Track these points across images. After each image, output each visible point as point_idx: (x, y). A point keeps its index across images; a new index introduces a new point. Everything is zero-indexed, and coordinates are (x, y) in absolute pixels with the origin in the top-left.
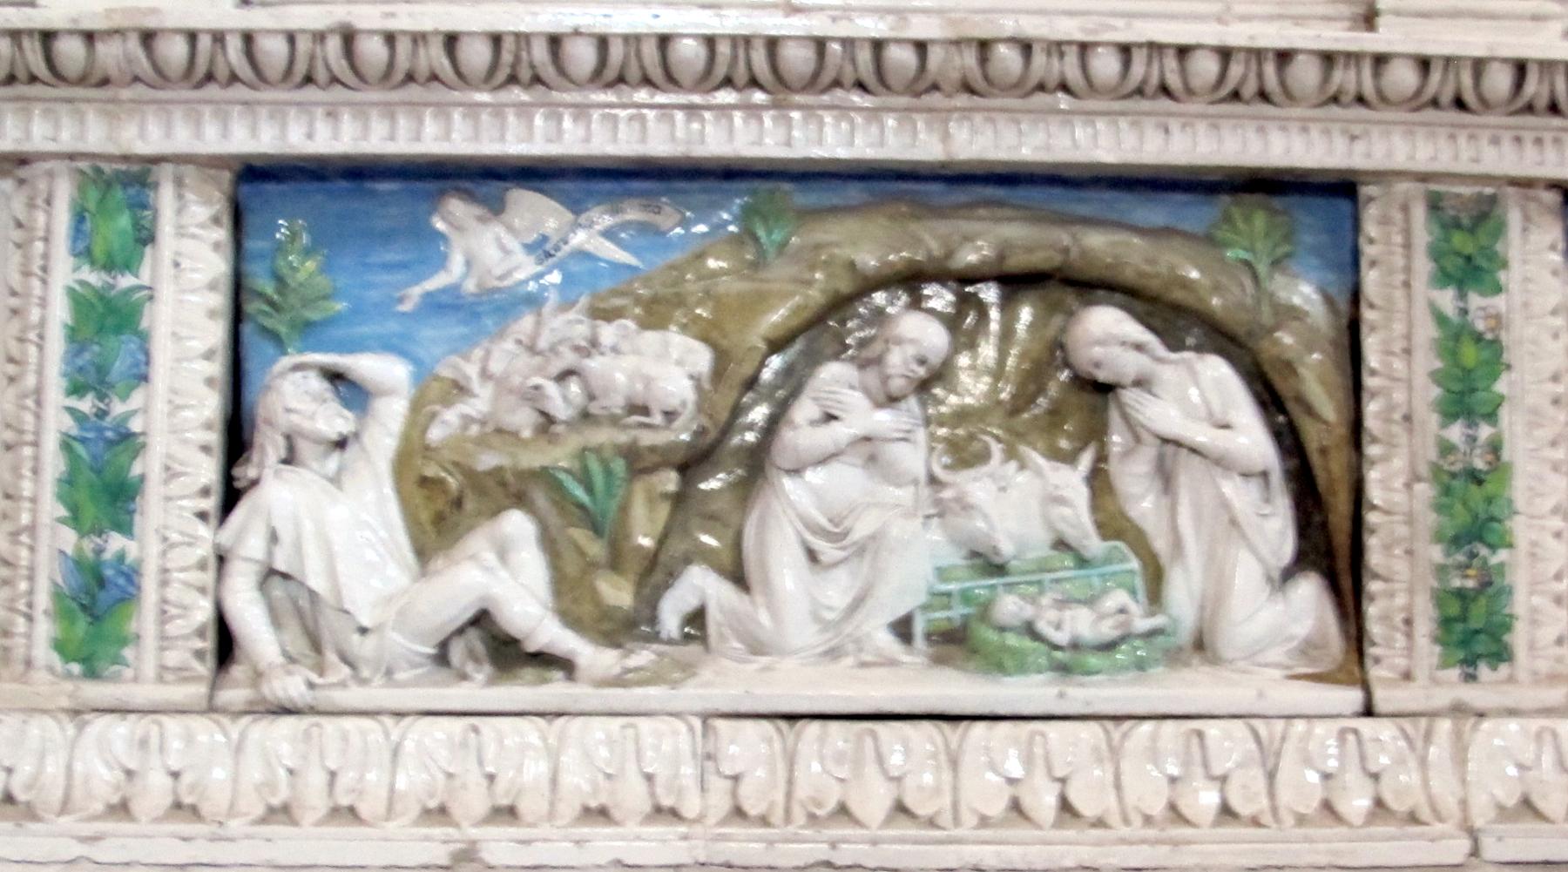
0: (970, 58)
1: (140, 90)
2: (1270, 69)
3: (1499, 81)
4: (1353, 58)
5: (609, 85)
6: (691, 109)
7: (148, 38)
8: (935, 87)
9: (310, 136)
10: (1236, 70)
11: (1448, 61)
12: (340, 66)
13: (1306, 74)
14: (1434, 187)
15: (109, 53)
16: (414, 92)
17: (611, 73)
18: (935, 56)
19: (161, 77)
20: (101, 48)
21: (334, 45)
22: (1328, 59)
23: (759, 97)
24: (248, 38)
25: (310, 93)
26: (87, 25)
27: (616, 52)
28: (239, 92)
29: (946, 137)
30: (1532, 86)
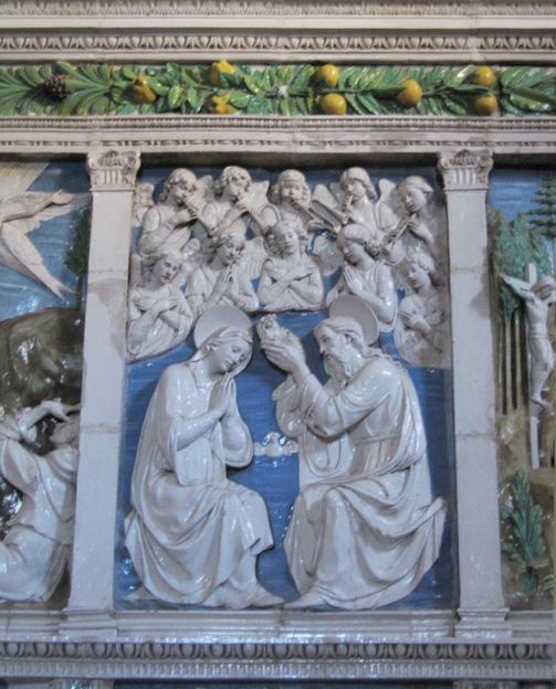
0: (331, 649)
1: (89, 660)
2: (420, 650)
3: (491, 651)
4: (446, 646)
5: (226, 658)
6: (250, 664)
7: (93, 645)
8: (321, 657)
9: (138, 672)
10: (410, 650)
11: (474, 646)
12: (148, 652)
13: (432, 651)
14: (476, 682)
15: (81, 649)
16: (169, 660)
17: (227, 654)
18: (321, 649)
19: (96, 656)
20: (79, 648)
21: (147, 647)
22: (438, 646)
23: (270, 661)
24: (122, 645)
25: (139, 660)
26: (76, 641)
27: (228, 649)
28: (119, 660)
29: (325, 672)
30: (501, 652)
